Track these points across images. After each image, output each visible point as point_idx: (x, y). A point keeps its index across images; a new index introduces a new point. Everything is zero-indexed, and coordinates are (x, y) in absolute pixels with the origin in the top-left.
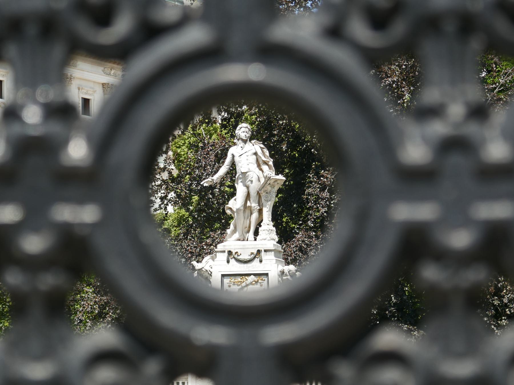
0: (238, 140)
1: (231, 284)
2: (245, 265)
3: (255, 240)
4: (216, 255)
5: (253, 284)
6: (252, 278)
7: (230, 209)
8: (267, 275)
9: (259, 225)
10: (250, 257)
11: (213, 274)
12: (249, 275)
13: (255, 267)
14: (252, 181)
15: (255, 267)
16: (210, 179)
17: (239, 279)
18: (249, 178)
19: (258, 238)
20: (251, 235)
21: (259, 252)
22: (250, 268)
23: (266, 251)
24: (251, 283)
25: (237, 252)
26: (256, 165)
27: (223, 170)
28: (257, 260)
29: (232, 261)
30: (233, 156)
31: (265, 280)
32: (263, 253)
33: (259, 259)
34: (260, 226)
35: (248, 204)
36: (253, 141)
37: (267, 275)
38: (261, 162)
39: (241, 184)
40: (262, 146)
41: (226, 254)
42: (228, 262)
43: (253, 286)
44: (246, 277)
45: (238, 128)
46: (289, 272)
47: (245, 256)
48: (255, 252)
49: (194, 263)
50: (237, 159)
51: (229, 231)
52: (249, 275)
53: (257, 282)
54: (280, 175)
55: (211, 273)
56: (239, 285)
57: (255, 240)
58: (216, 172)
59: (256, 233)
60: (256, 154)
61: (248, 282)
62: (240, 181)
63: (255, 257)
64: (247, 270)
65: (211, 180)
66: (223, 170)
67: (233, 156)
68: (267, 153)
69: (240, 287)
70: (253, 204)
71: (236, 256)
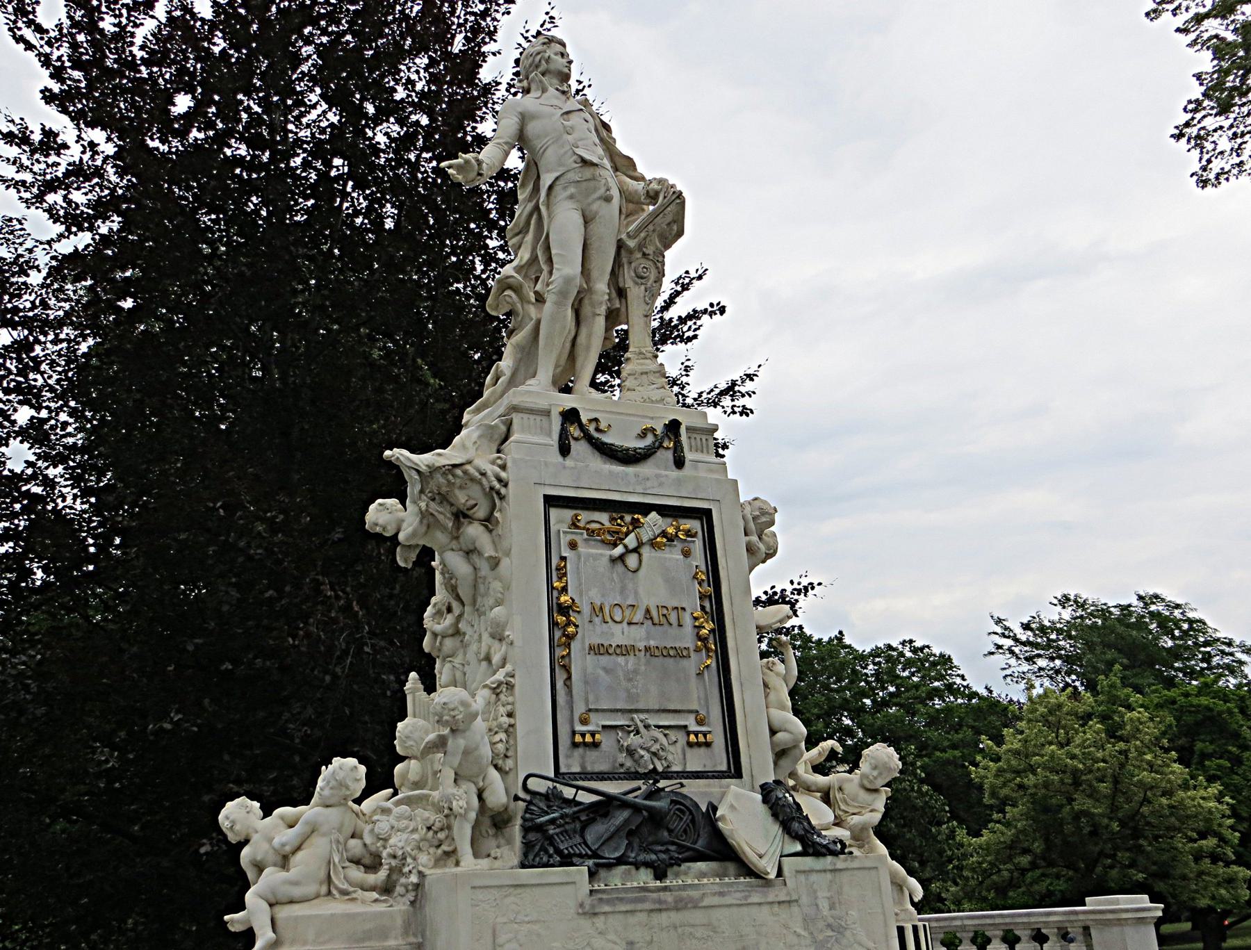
1: (578, 539)
2: (631, 470)
8: (704, 515)
10: (641, 444)
12: (646, 509)
14: (608, 199)
17: (604, 517)
18: (602, 191)
22: (649, 484)
25: (596, 420)
29: (579, 448)
33: (669, 455)
37: (704, 515)
39: (570, 205)
42: (565, 450)
51: (506, 364)
53: (670, 539)
55: (506, 485)
62: (561, 194)
69: (619, 550)
70: (602, 286)
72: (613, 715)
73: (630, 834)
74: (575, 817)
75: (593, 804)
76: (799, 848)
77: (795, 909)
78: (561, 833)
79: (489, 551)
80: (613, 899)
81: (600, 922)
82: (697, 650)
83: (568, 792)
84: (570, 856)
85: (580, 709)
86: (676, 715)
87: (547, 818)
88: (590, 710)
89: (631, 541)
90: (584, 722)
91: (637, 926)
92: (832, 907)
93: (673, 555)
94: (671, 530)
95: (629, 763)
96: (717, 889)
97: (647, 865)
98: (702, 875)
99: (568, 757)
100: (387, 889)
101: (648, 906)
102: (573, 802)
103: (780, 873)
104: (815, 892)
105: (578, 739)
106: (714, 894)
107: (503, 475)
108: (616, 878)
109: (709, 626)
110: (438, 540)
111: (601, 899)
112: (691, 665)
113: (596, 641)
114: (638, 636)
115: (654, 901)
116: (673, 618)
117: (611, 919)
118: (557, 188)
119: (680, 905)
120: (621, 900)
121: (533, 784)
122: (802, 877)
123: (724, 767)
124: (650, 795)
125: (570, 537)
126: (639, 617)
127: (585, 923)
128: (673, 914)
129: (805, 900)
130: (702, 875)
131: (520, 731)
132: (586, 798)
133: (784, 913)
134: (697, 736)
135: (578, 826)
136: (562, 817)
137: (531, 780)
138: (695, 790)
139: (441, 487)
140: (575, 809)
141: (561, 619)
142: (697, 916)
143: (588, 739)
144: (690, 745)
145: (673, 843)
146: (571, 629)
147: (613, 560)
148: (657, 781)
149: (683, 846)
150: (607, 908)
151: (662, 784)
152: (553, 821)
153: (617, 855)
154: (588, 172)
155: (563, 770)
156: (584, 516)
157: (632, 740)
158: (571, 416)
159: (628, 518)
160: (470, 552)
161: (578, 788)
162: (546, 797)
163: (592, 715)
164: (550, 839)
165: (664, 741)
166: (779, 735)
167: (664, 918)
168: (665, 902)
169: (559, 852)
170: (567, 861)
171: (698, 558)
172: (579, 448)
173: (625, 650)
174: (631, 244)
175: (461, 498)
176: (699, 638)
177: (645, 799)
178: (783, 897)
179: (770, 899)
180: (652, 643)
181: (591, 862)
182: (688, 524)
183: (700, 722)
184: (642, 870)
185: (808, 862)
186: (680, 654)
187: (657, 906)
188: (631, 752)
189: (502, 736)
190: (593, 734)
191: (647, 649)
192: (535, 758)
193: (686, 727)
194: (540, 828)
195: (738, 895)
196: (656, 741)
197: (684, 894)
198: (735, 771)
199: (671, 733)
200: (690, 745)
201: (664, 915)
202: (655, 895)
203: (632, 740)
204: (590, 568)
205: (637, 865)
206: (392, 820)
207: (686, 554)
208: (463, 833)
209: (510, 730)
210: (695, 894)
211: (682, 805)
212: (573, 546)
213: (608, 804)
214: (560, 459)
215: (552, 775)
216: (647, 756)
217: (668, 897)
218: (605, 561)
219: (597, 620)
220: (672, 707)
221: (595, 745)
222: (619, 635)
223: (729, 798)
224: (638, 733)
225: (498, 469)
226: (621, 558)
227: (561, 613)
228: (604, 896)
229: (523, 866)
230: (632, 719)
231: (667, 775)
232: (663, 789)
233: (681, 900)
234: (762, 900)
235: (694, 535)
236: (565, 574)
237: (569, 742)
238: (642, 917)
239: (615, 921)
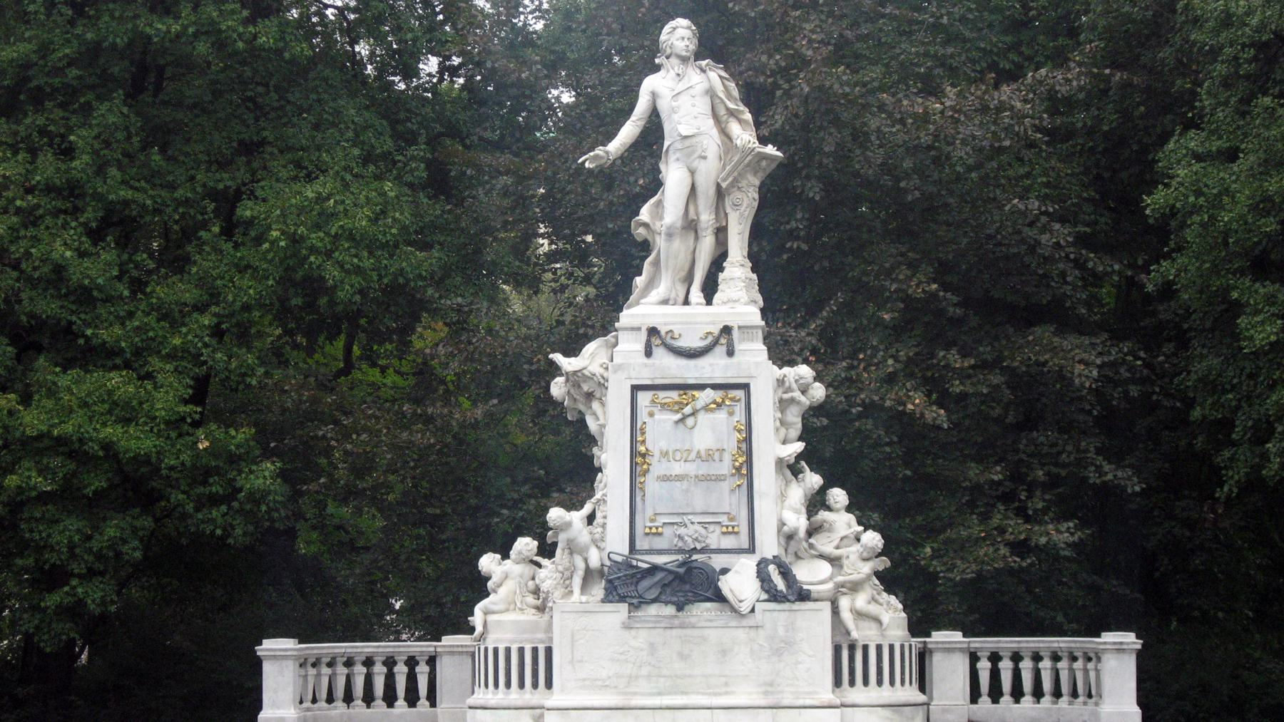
0: (668, 58)
2: (692, 363)
3: (709, 302)
4: (616, 337)
5: (712, 410)
6: (706, 396)
7: (646, 225)
8: (746, 387)
9: (717, 264)
10: (702, 344)
11: (610, 385)
12: (701, 387)
13: (714, 368)
15: (714, 368)
16: (599, 151)
17: (674, 395)
18: (699, 152)
19: (717, 298)
20: (696, 295)
21: (727, 330)
23: (740, 327)
24: (706, 408)
26: (711, 122)
27: (628, 132)
28: (720, 350)
30: (654, 95)
31: (739, 400)
32: (735, 333)
33: (724, 348)
34: (722, 269)
35: (692, 215)
36: (704, 63)
37: (746, 387)
38: (722, 112)
40: (723, 74)
41: (643, 335)
42: (648, 353)
43: (711, 416)
44: (696, 393)
45: (667, 29)
46: (796, 381)
47: (694, 342)
48: (716, 332)
49: (557, 357)
50: (663, 106)
51: (639, 281)
52: (701, 387)
54: (770, 146)
56: (677, 412)
57: (709, 302)
58: (610, 136)
59: (710, 289)
60: (711, 93)
61: (699, 404)
62: (672, 157)
63: (716, 343)
64: (697, 375)
65: (601, 153)
66: (628, 132)
67: (654, 95)
68: (736, 93)
69: (679, 416)
70: (707, 218)
71: (669, 341)
74: (633, 576)
75: (648, 569)
77: (760, 630)
79: (602, 421)
81: (633, 632)
82: (733, 475)
83: (634, 563)
85: (649, 513)
89: (688, 410)
90: (652, 521)
91: (657, 636)
92: (787, 631)
93: (722, 415)
94: (719, 400)
97: (673, 603)
98: (708, 610)
100: (541, 609)
101: (663, 625)
102: (637, 567)
103: (753, 610)
105: (647, 530)
107: (605, 375)
108: (653, 610)
109: (741, 460)
110: (582, 407)
112: (726, 486)
113: (662, 473)
114: (691, 469)
116: (717, 456)
117: (641, 631)
118: (671, 152)
119: (682, 627)
123: (746, 546)
125: (648, 410)
126: (693, 456)
127: (626, 634)
129: (768, 626)
130: (708, 610)
131: (609, 527)
133: (753, 633)
135: (635, 580)
139: (575, 379)
141: (639, 460)
142: (695, 632)
143: (654, 530)
144: (724, 533)
146: (645, 467)
147: (677, 422)
151: (695, 557)
154: (687, 143)
155: (638, 548)
156: (662, 394)
157: (682, 531)
158: (653, 331)
159: (690, 393)
160: (598, 419)
164: (615, 588)
165: (703, 531)
166: (786, 528)
167: (674, 632)
170: (622, 599)
171: (740, 415)
172: (659, 352)
173: (680, 478)
174: (724, 185)
175: (585, 388)
176: (734, 467)
180: (700, 473)
181: (635, 601)
182: (732, 393)
183: (731, 520)
186: (719, 478)
188: (680, 537)
189: (600, 530)
191: (696, 477)
192: (617, 543)
198: (751, 550)
199: (711, 528)
200: (724, 533)
203: (682, 531)
204: (660, 428)
205: (667, 603)
206: (548, 573)
207: (731, 414)
208: (577, 581)
209: (604, 526)
210: (693, 620)
212: (651, 415)
213: (654, 569)
214: (645, 360)
215: (626, 552)
216: (689, 540)
217: (676, 622)
218: (671, 423)
219: (663, 460)
222: (678, 468)
225: (602, 371)
226: (682, 420)
227: (638, 460)
229: (603, 601)
231: (703, 551)
235: (739, 400)
236: (643, 434)
238: (661, 631)
239: (643, 634)
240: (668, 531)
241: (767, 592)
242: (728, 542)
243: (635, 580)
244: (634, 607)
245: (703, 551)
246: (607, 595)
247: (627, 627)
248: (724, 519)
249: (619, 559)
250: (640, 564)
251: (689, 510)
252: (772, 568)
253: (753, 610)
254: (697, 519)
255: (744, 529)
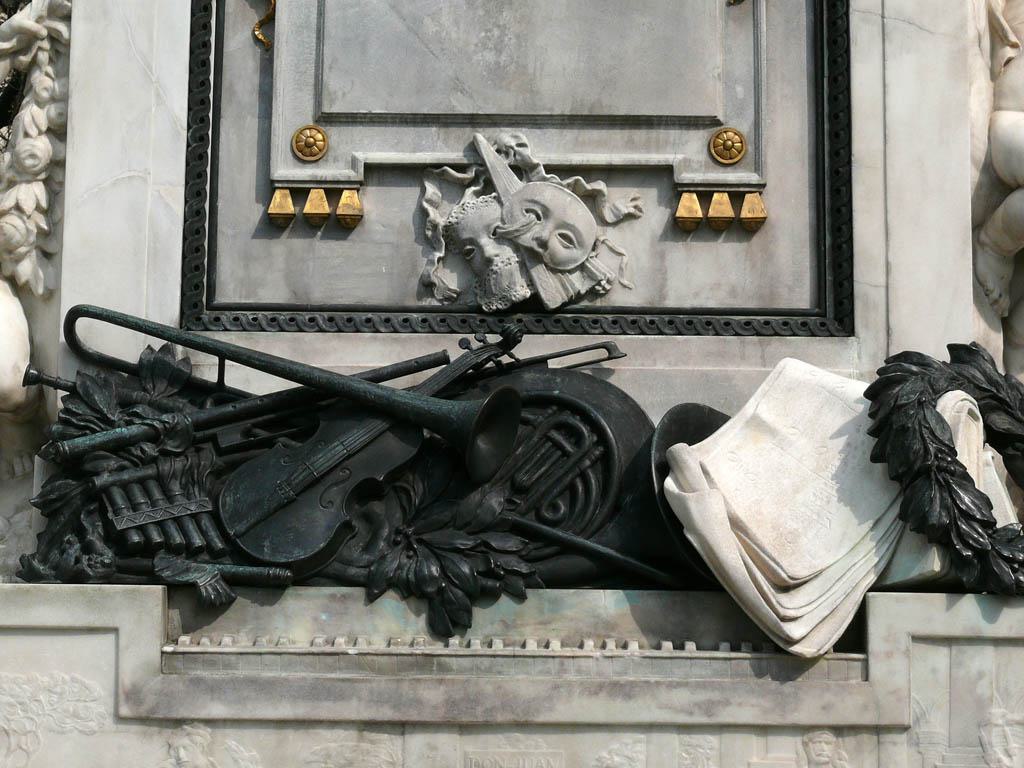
72: (409, 133)
73: (366, 492)
74: (197, 438)
76: (934, 563)
78: (142, 482)
80: (235, 683)
83: (207, 369)
84: (148, 549)
85: (292, 112)
86: (640, 135)
87: (99, 438)
88: (325, 119)
95: (450, 280)
96: (610, 671)
97: (411, 590)
99: (247, 259)
102: (220, 392)
103: (855, 639)
104: (982, 704)
105: (282, 203)
106: (597, 689)
108: (302, 621)
111: (197, 682)
115: (378, 700)
120: (266, 688)
121: (100, 338)
122: (940, 656)
124: (461, 383)
128: (447, 741)
129: (937, 725)
130: (602, 630)
132: (262, 385)
134: (705, 194)
135: (208, 458)
136: (154, 437)
137: (82, 325)
138: (653, 375)
140: (210, 410)
143: (316, 203)
145: (517, 529)
148: (509, 343)
149: (551, 540)
150: (217, 710)
151: (530, 347)
152: (119, 447)
153: (299, 554)
155: (229, 291)
161: (224, 354)
162: (137, 373)
163: (335, 133)
164: (99, 499)
165: (579, 214)
168: (418, 702)
169: (116, 539)
170: (133, 563)
177: (437, 394)
178: (849, 711)
179: (802, 717)
184: (390, 601)
185: (968, 612)
187: (386, 713)
188: (458, 246)
190: (333, 193)
193: (667, 170)
194: (73, 466)
195: (681, 697)
196: (544, 214)
197: (486, 685)
201: (417, 741)
202: (382, 683)
203: (473, 211)
205: (373, 588)
210: (524, 684)
211: (577, 411)
213: (317, 402)
215: (167, 312)
217: (432, 696)
220: (622, 110)
221: (342, 226)
223: (759, 405)
224: (488, 187)
228: (218, 675)
230: (473, 148)
231: (574, 316)
232: (542, 361)
233: (474, 701)
234: (773, 719)
237: (256, 213)
240: (385, 211)
241: (941, 537)
242: (706, 275)
243: (208, 458)
244: (196, 609)
245: (574, 316)
246: (49, 541)
247: (149, 715)
248: (687, 154)
249: (127, 347)
250: (239, 377)
251: (508, 104)
252: (955, 405)
253: (855, 639)
254: (542, 148)
255: (787, 201)
